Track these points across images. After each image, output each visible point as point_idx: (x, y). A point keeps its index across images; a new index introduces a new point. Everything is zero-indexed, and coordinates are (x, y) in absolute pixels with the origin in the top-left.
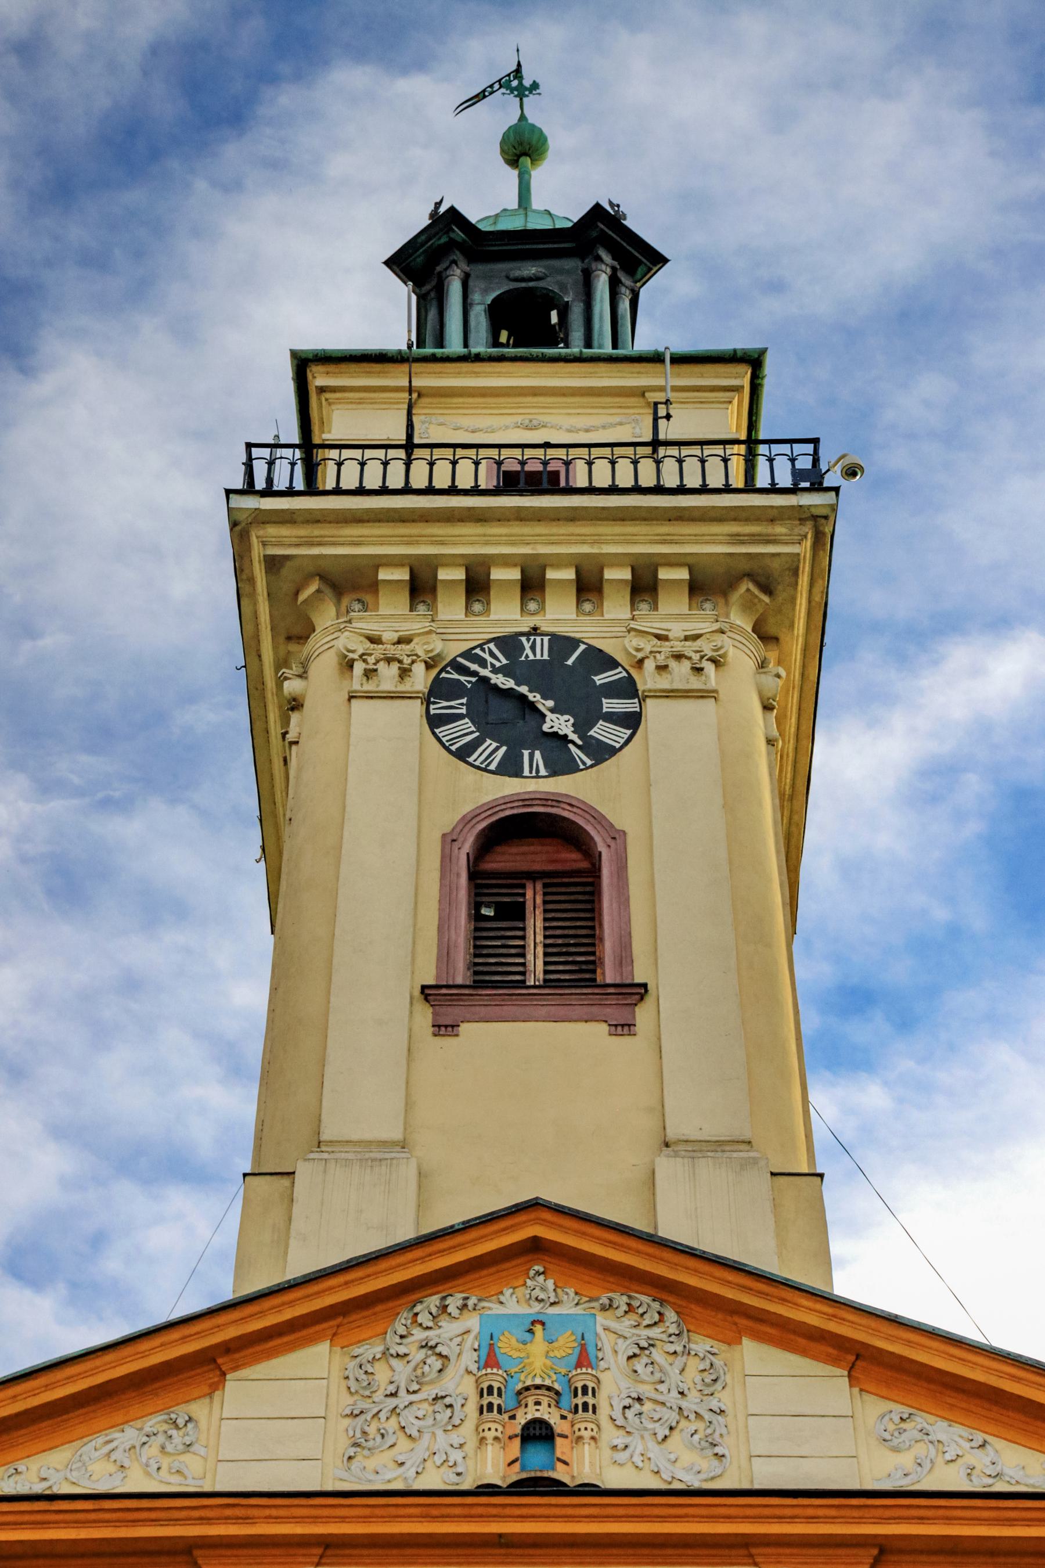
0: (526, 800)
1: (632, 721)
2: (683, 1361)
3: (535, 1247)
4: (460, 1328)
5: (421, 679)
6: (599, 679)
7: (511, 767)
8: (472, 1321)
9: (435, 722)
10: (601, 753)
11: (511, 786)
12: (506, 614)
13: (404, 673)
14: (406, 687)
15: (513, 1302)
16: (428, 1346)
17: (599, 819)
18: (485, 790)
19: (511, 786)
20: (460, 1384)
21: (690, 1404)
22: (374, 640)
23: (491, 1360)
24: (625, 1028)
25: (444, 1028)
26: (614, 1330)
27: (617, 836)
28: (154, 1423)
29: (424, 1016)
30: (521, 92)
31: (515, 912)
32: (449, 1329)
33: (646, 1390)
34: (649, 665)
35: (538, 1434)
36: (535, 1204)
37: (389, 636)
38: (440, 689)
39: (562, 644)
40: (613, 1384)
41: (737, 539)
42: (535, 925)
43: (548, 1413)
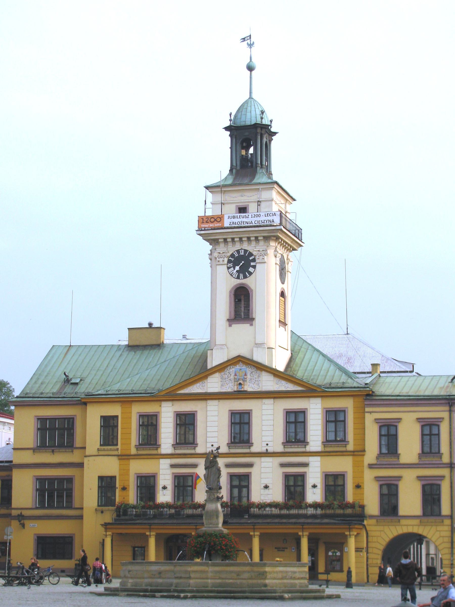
0: (240, 284)
1: (254, 267)
2: (256, 374)
3: (240, 361)
4: (232, 370)
5: (226, 260)
6: (251, 258)
7: (238, 278)
8: (234, 369)
9: (229, 268)
10: (250, 274)
11: (239, 281)
12: (238, 246)
13: (223, 261)
14: (224, 263)
15: (238, 367)
16: (229, 372)
17: (250, 288)
18: (236, 282)
19: (239, 281)
20: (232, 377)
21: (257, 379)
22: (219, 253)
23: (236, 375)
24: (251, 325)
25: (230, 326)
26: (249, 370)
27: (252, 291)
28: (201, 383)
29: (228, 323)
30: (250, 45)
31: (240, 300)
32: (231, 370)
33: (252, 378)
34: (257, 256)
35: (240, 384)
36: (239, 356)
37: (221, 252)
38: (229, 261)
39: (246, 251)
40: (249, 376)
41: (268, 233)
42: (243, 302)
43: (241, 382)
